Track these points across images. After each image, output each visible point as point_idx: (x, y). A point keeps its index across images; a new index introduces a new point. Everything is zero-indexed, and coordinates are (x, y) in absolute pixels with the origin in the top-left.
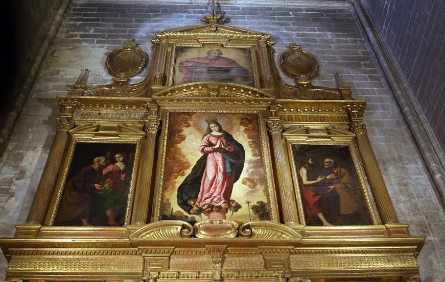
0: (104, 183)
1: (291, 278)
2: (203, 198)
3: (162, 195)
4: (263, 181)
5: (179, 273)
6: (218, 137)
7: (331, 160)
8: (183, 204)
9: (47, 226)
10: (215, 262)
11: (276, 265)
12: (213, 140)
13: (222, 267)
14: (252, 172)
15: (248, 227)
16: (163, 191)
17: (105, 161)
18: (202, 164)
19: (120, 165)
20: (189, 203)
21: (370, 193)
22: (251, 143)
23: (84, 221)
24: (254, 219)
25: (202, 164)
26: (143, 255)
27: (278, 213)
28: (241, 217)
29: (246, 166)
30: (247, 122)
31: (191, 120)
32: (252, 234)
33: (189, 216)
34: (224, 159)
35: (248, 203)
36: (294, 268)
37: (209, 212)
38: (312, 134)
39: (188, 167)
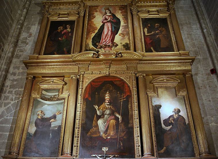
0: (62, 37)
1: (137, 73)
3: (86, 41)
4: (128, 34)
5: (92, 72)
6: (109, 16)
7: (158, 24)
8: (94, 44)
9: (41, 55)
10: (107, 68)
11: (132, 68)
12: (107, 17)
13: (109, 70)
14: (123, 31)
15: (120, 53)
16: (86, 40)
17: (63, 28)
18: (102, 28)
19: (69, 30)
21: (174, 38)
22: (123, 18)
23: (55, 53)
24: (123, 50)
25: (102, 28)
26: (78, 65)
27: (134, 48)
28: (117, 49)
29: (121, 28)
30: (122, 9)
32: (122, 56)
33: (97, 49)
34: (111, 25)
35: (121, 43)
36: (139, 70)
37: (105, 48)
38: (150, 13)
39: (96, 29)
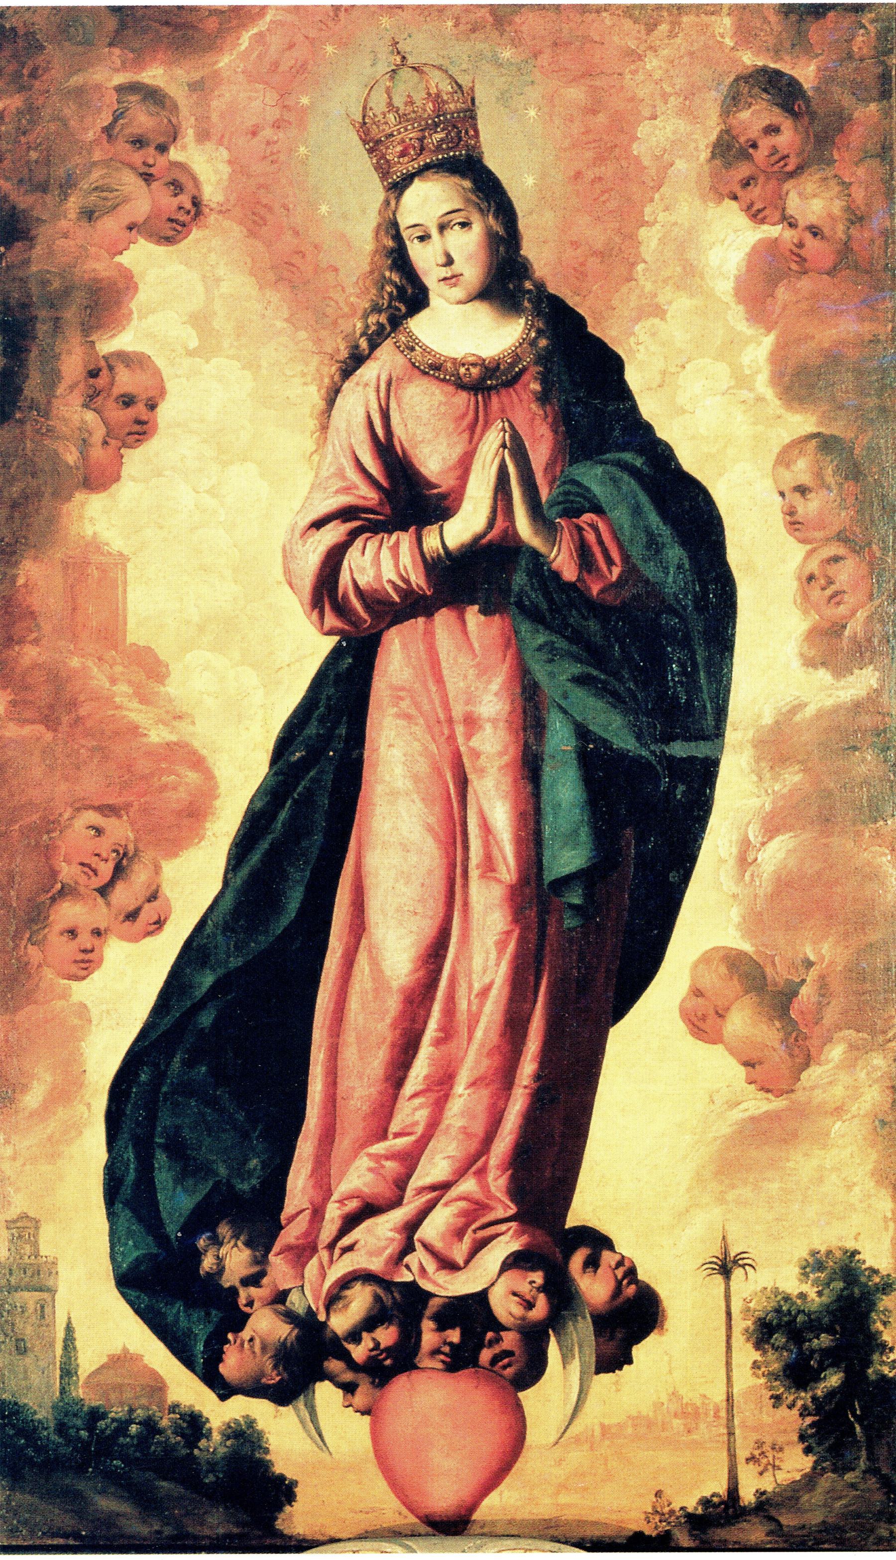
2: (333, 1213)
20: (208, 1263)
31: (203, 136)
